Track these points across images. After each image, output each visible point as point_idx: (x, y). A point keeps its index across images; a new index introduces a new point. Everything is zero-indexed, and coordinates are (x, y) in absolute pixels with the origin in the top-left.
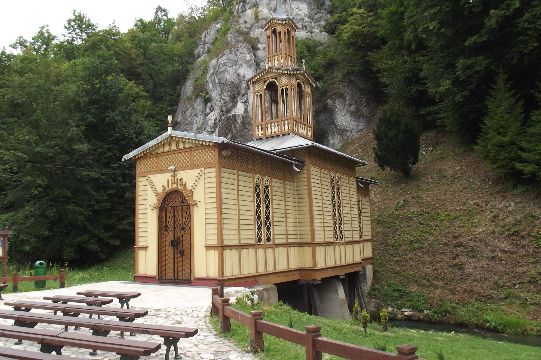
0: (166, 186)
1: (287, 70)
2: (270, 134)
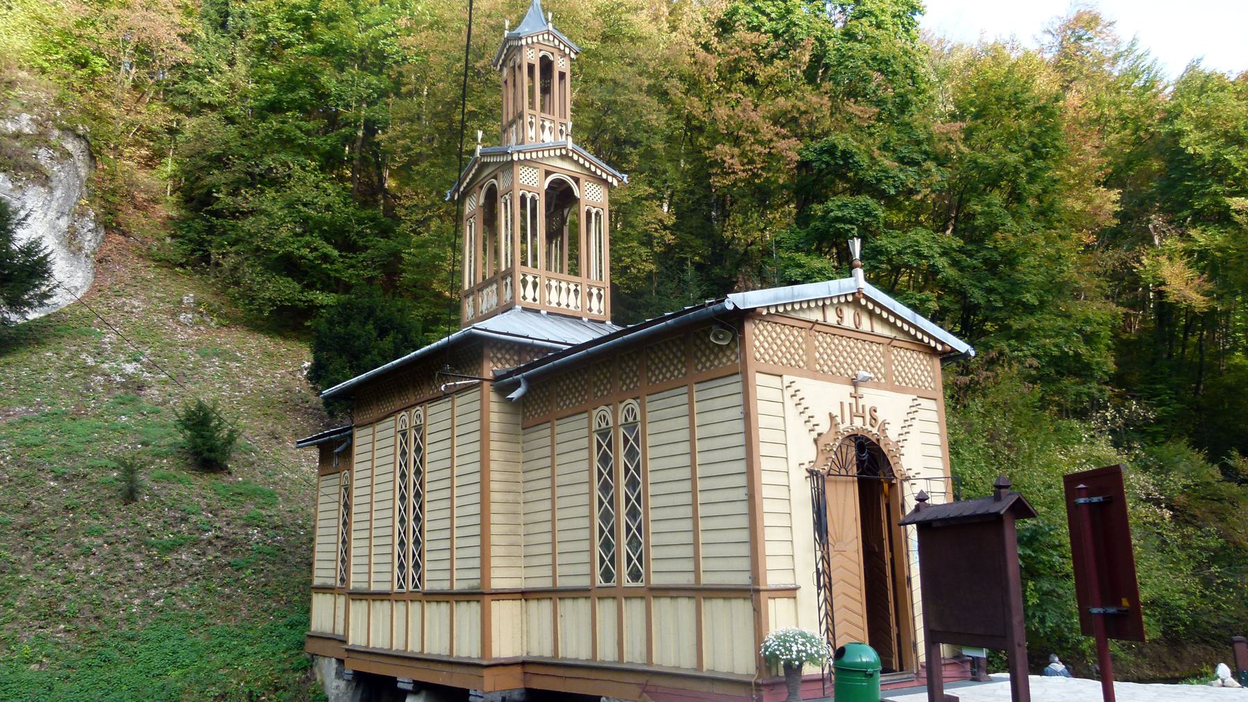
0: (839, 419)
1: (614, 176)
2: (554, 305)
